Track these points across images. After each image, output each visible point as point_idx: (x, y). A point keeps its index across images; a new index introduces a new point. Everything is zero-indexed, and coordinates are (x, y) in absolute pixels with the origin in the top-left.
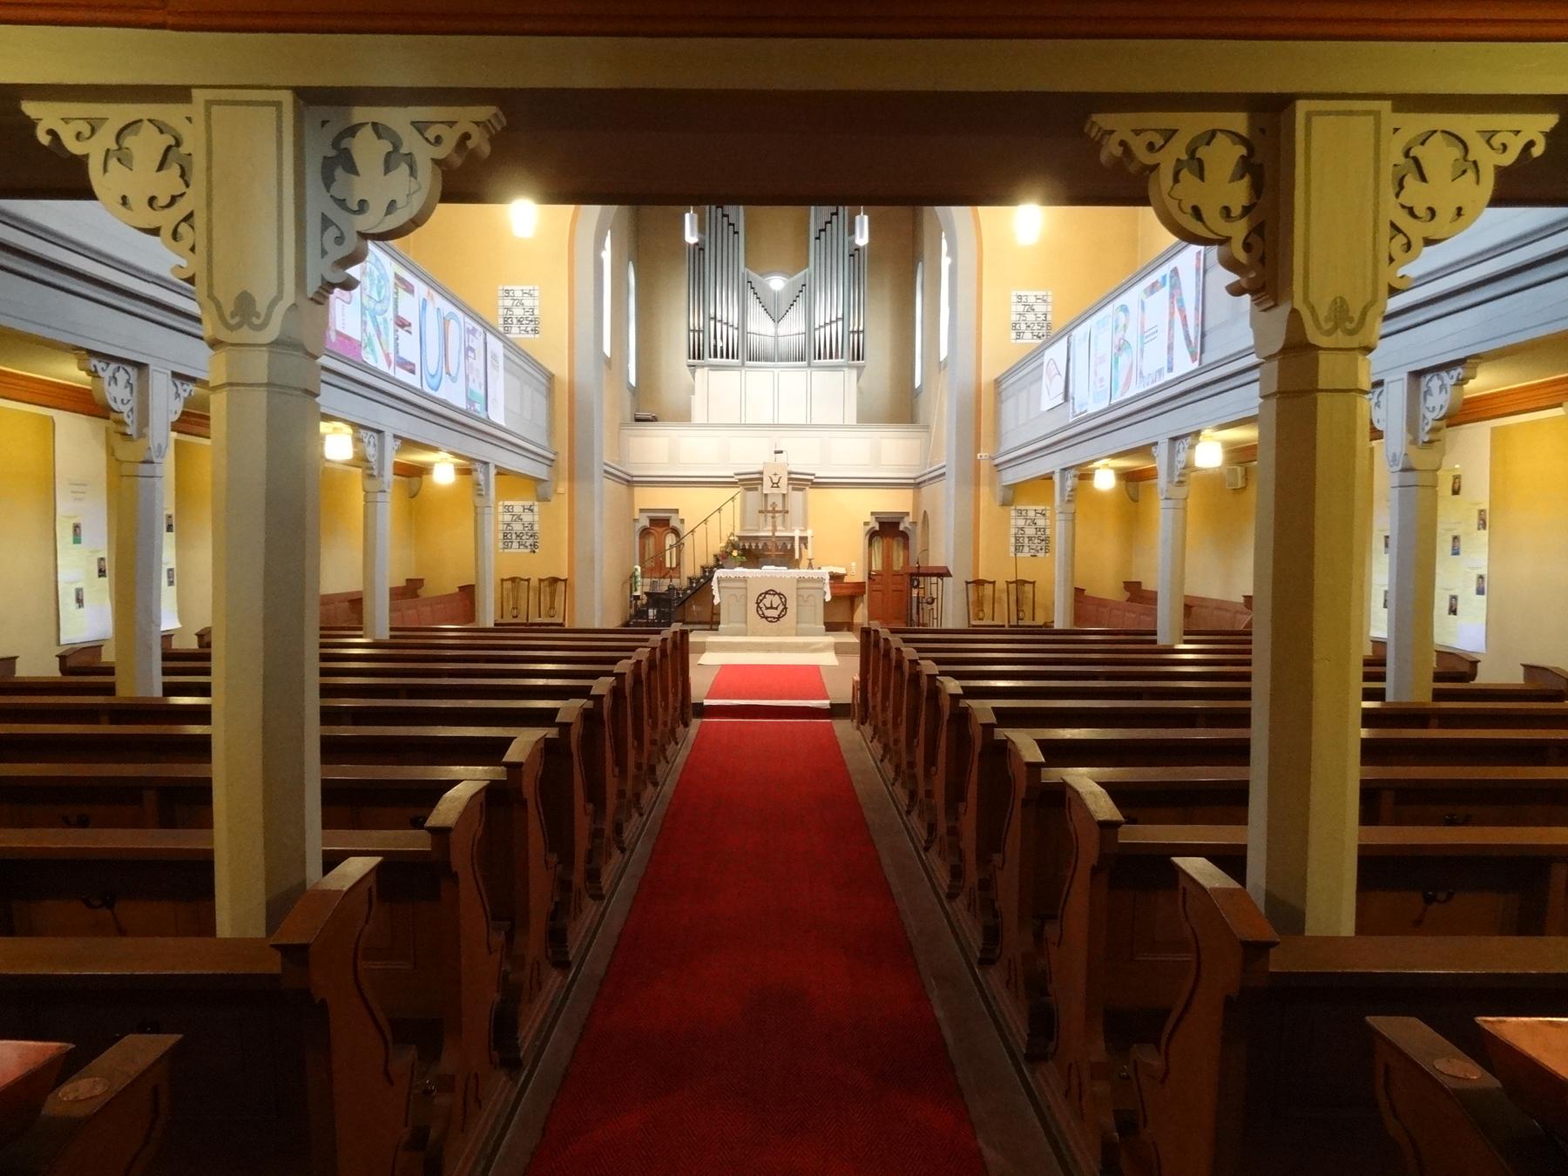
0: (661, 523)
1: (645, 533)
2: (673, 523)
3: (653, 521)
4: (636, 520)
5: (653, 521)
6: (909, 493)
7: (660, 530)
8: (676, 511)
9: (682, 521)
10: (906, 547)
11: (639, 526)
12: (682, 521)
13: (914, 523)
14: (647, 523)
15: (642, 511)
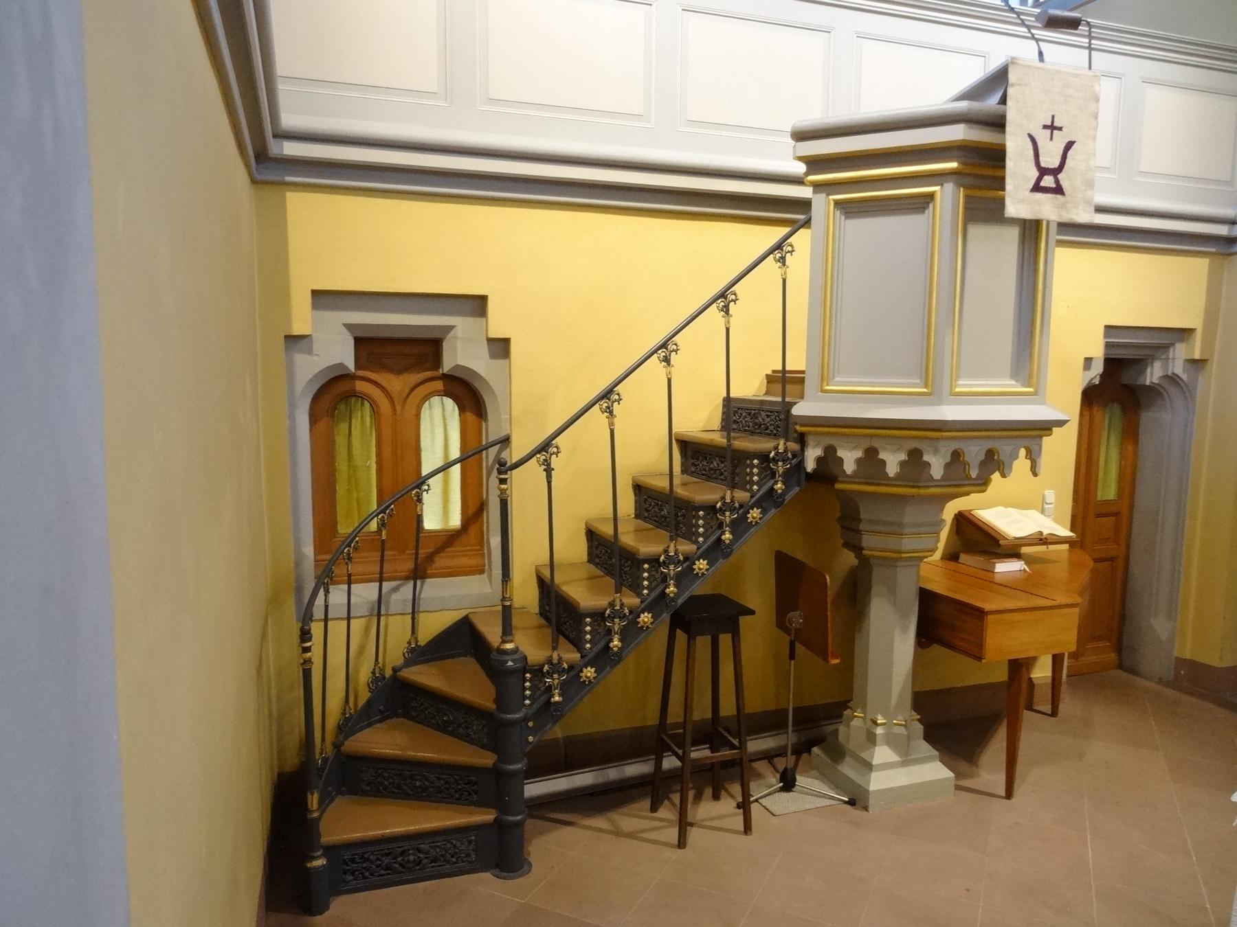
0: (407, 353)
1: (334, 395)
2: (464, 352)
3: (371, 347)
4: (294, 341)
5: (371, 347)
6: (1192, 271)
7: (396, 383)
8: (477, 305)
9: (501, 347)
10: (1131, 433)
11: (309, 369)
12: (501, 347)
13: (1197, 364)
14: (343, 354)
15: (321, 298)
